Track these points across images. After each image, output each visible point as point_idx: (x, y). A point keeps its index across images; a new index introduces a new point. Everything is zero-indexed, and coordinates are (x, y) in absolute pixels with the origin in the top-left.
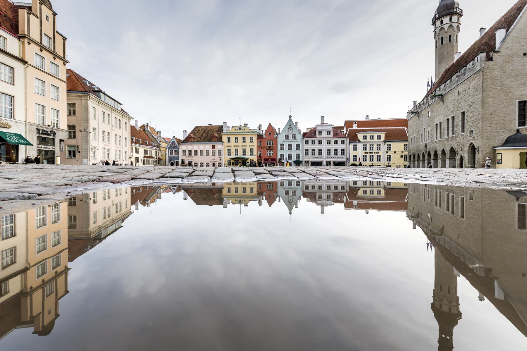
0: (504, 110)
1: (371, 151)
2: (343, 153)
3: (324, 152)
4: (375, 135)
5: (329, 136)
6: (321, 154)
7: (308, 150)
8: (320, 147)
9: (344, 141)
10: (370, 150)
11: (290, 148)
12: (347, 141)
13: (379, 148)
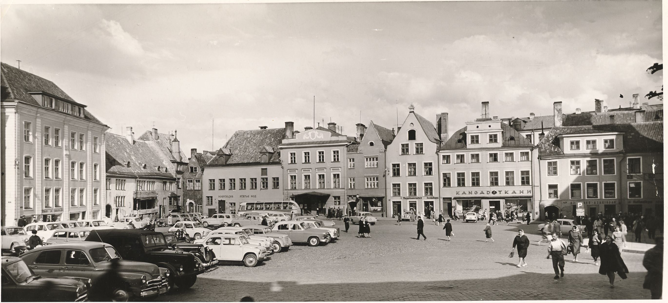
2: (525, 181)
3: (485, 180)
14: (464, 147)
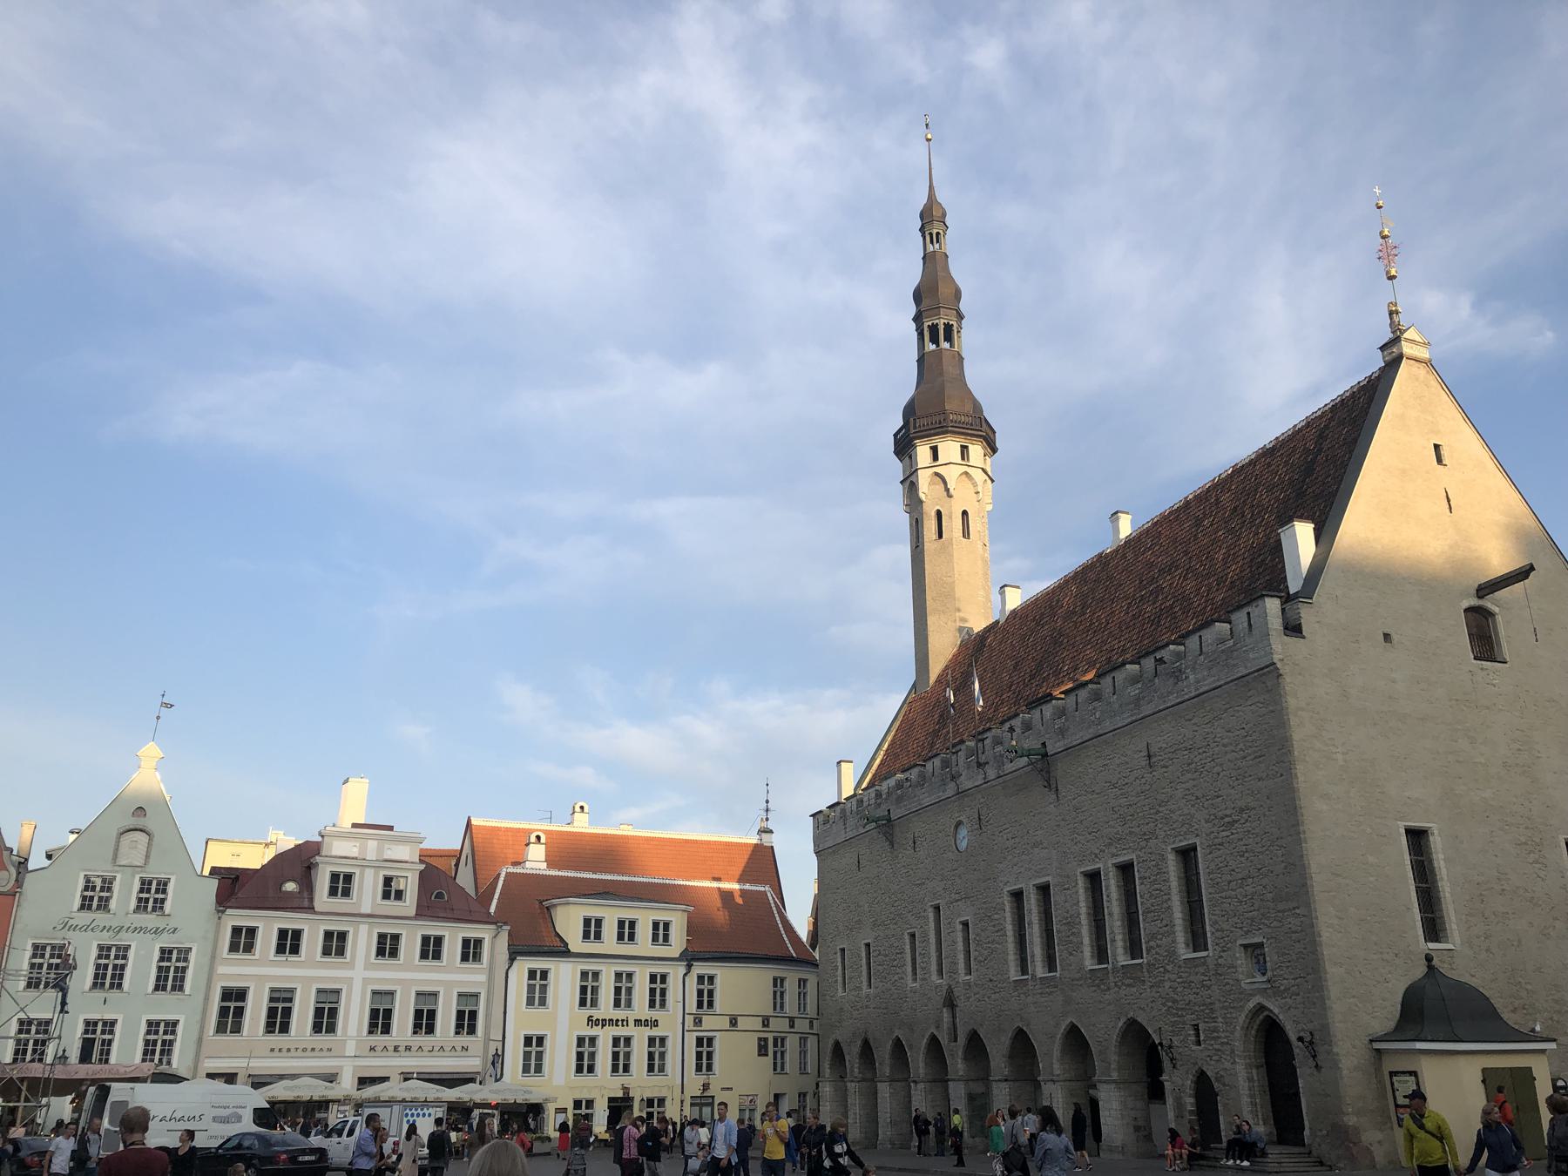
0: (1371, 859)
1: (619, 1014)
2: (466, 1021)
3: (354, 1016)
4: (645, 917)
5: (392, 906)
6: (331, 1029)
7: (241, 994)
8: (328, 973)
9: (479, 942)
10: (617, 1004)
11: (109, 975)
12: (495, 942)
13: (657, 997)
14: (303, 902)
